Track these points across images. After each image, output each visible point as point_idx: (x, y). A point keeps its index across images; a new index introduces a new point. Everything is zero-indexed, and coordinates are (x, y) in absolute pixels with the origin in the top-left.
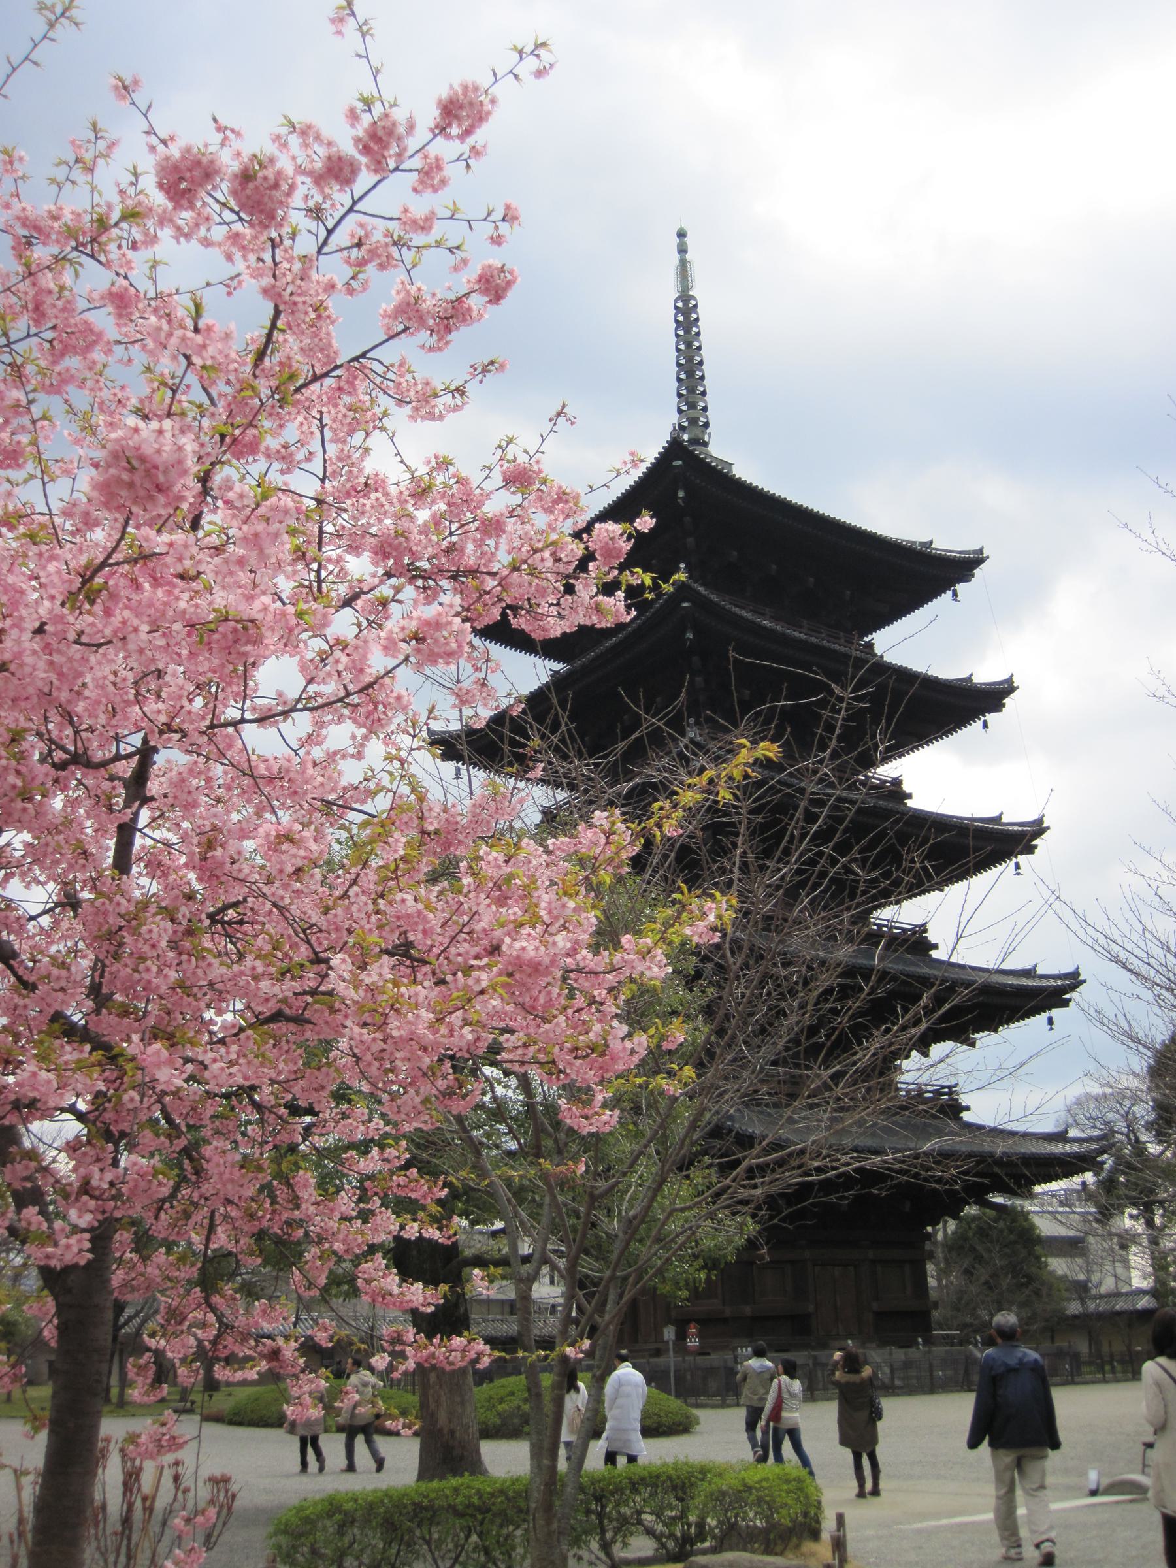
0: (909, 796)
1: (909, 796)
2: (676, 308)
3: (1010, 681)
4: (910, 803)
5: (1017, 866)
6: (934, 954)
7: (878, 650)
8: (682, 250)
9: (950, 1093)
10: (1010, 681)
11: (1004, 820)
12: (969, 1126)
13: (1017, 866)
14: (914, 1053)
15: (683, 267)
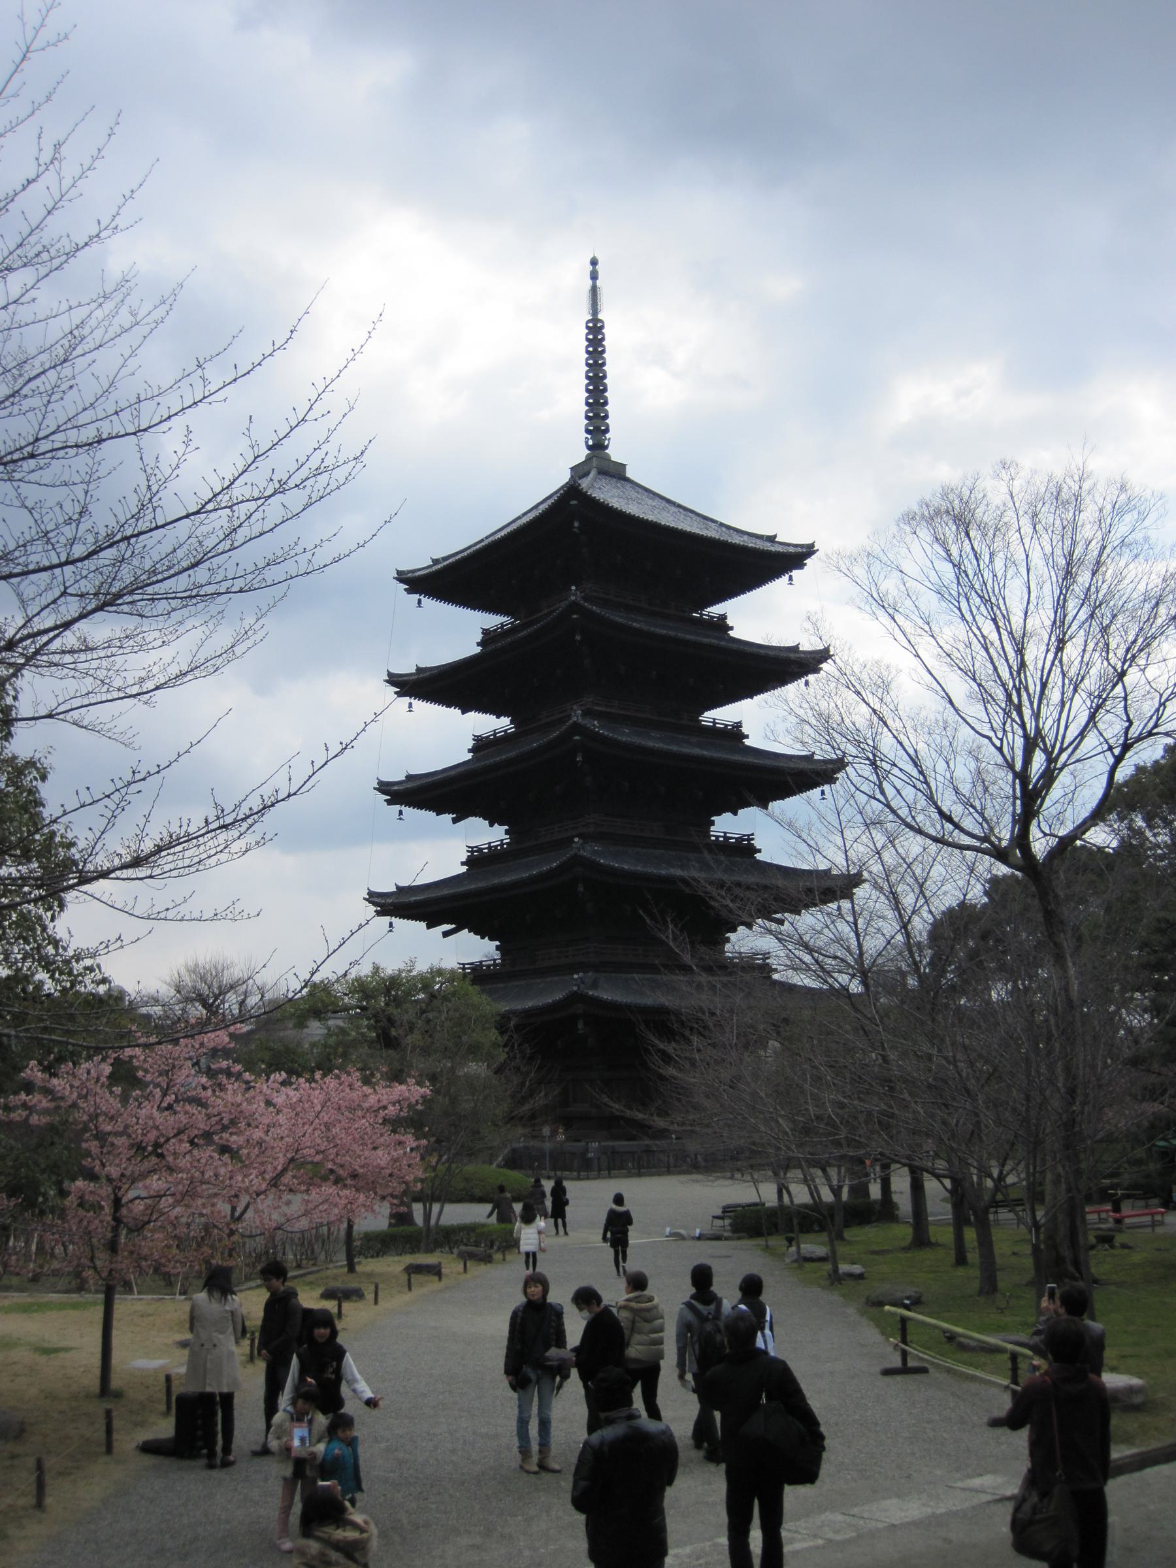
0: (747, 737)
1: (747, 737)
2: (588, 327)
3: (827, 650)
4: (747, 742)
5: (823, 793)
6: (758, 856)
7: (729, 622)
8: (594, 276)
9: (764, 959)
10: (827, 650)
11: (816, 757)
12: (776, 982)
13: (823, 793)
14: (741, 929)
15: (594, 290)
